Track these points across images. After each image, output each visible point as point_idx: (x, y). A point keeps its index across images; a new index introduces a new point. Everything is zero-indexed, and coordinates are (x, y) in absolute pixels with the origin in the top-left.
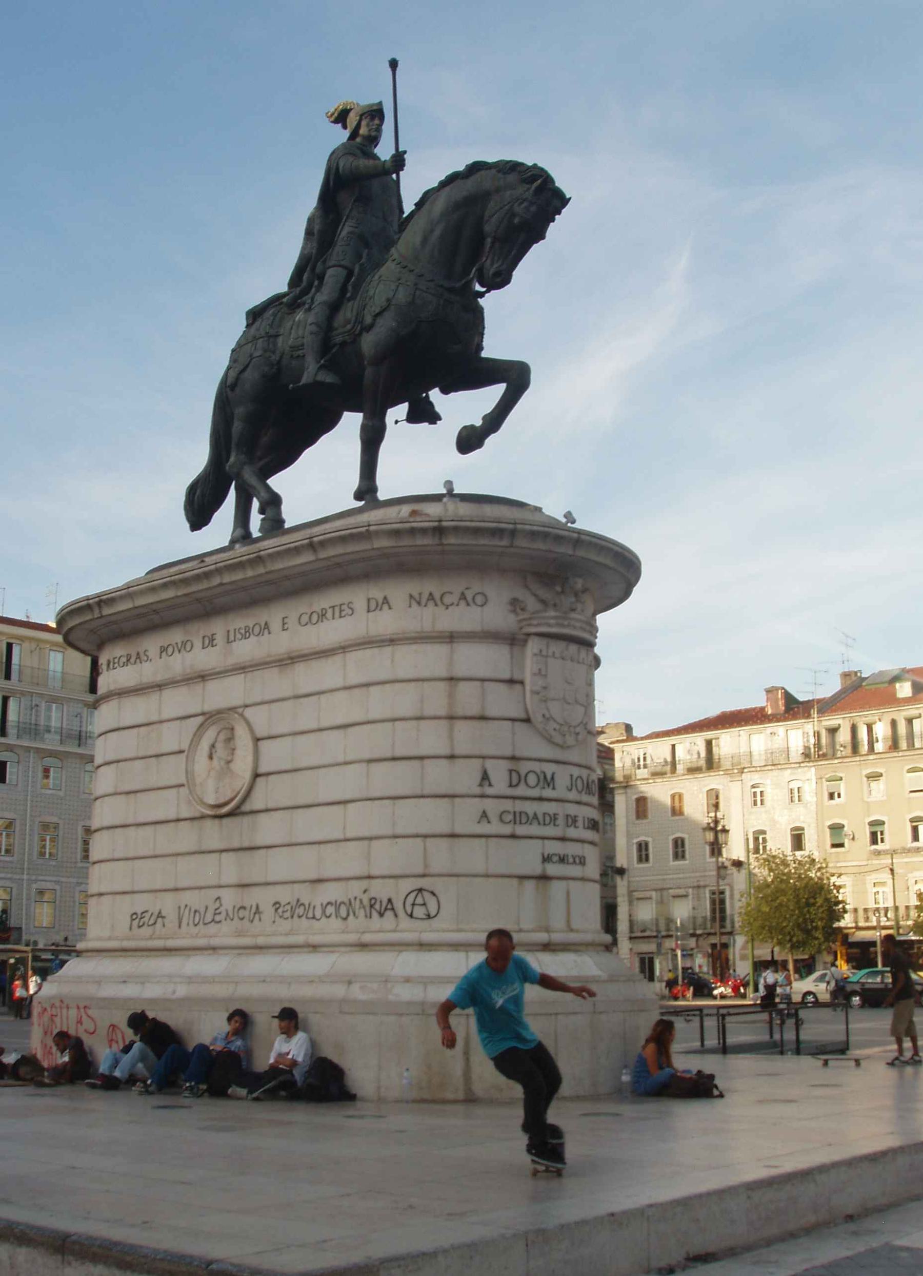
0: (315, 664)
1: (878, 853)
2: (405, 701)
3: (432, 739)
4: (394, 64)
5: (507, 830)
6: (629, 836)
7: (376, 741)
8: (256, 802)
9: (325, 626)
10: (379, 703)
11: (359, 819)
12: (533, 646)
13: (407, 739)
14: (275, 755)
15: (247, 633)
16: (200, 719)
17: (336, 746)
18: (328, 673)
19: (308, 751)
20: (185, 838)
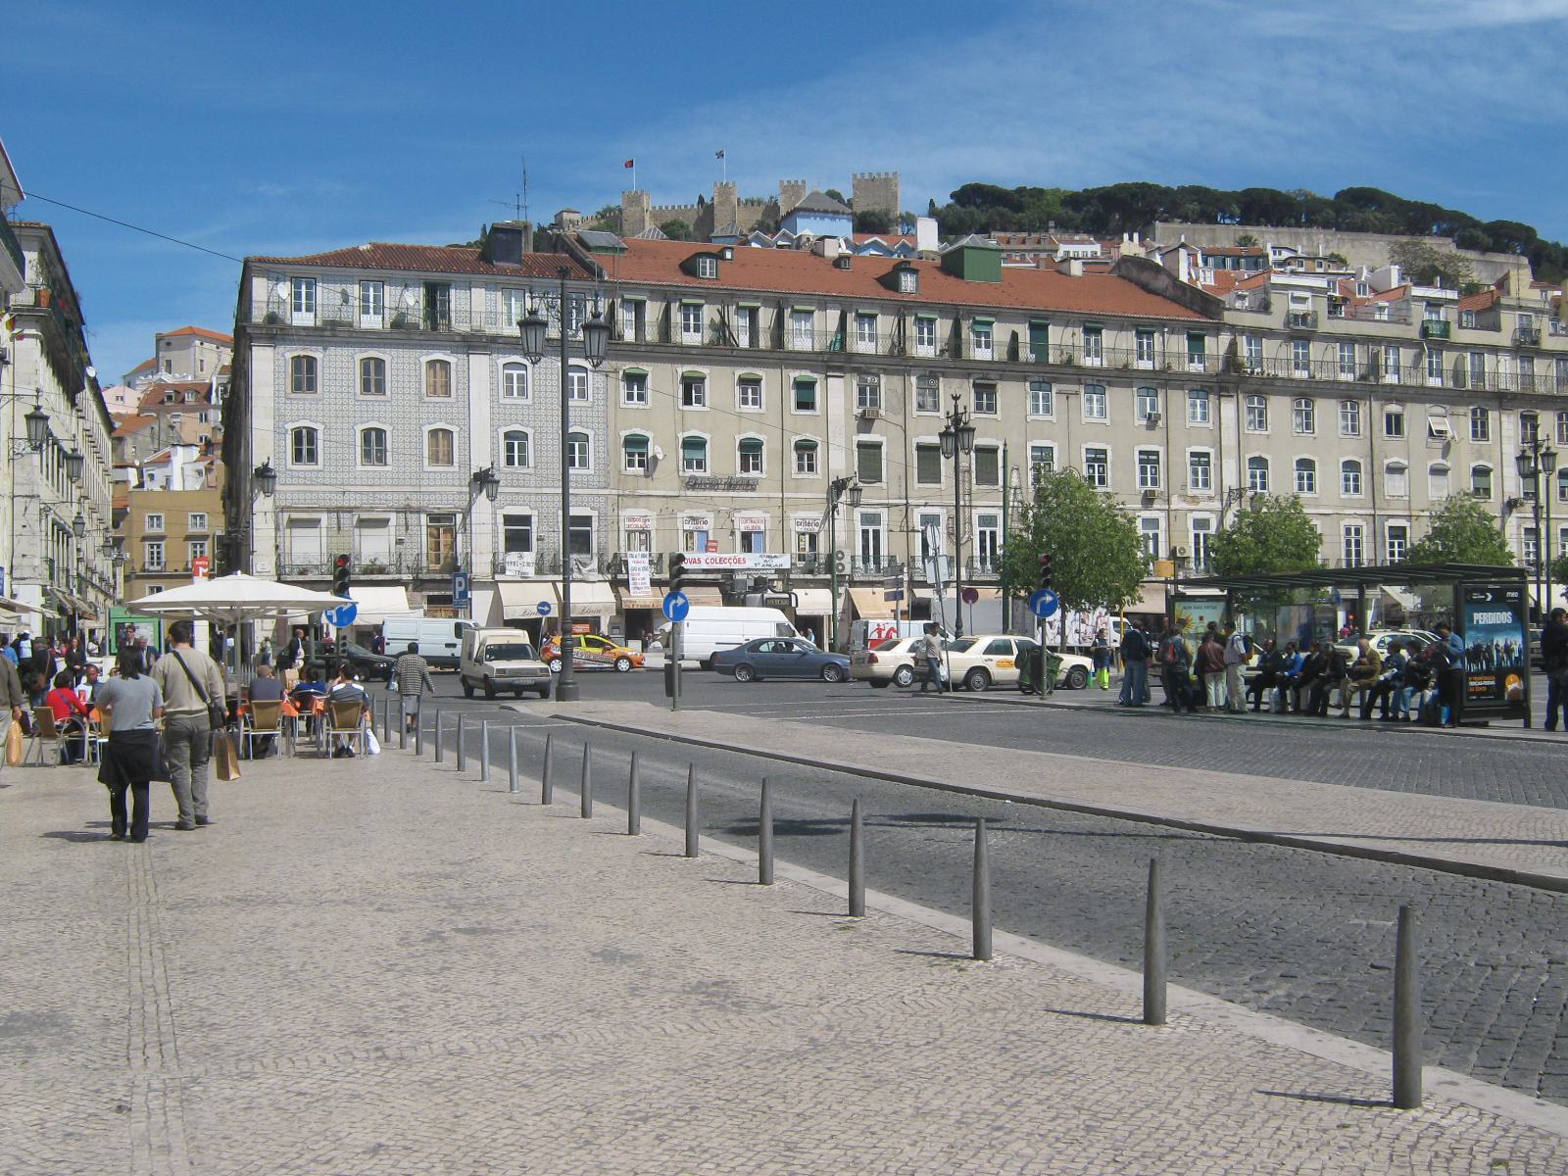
1: (693, 484)
6: (279, 417)
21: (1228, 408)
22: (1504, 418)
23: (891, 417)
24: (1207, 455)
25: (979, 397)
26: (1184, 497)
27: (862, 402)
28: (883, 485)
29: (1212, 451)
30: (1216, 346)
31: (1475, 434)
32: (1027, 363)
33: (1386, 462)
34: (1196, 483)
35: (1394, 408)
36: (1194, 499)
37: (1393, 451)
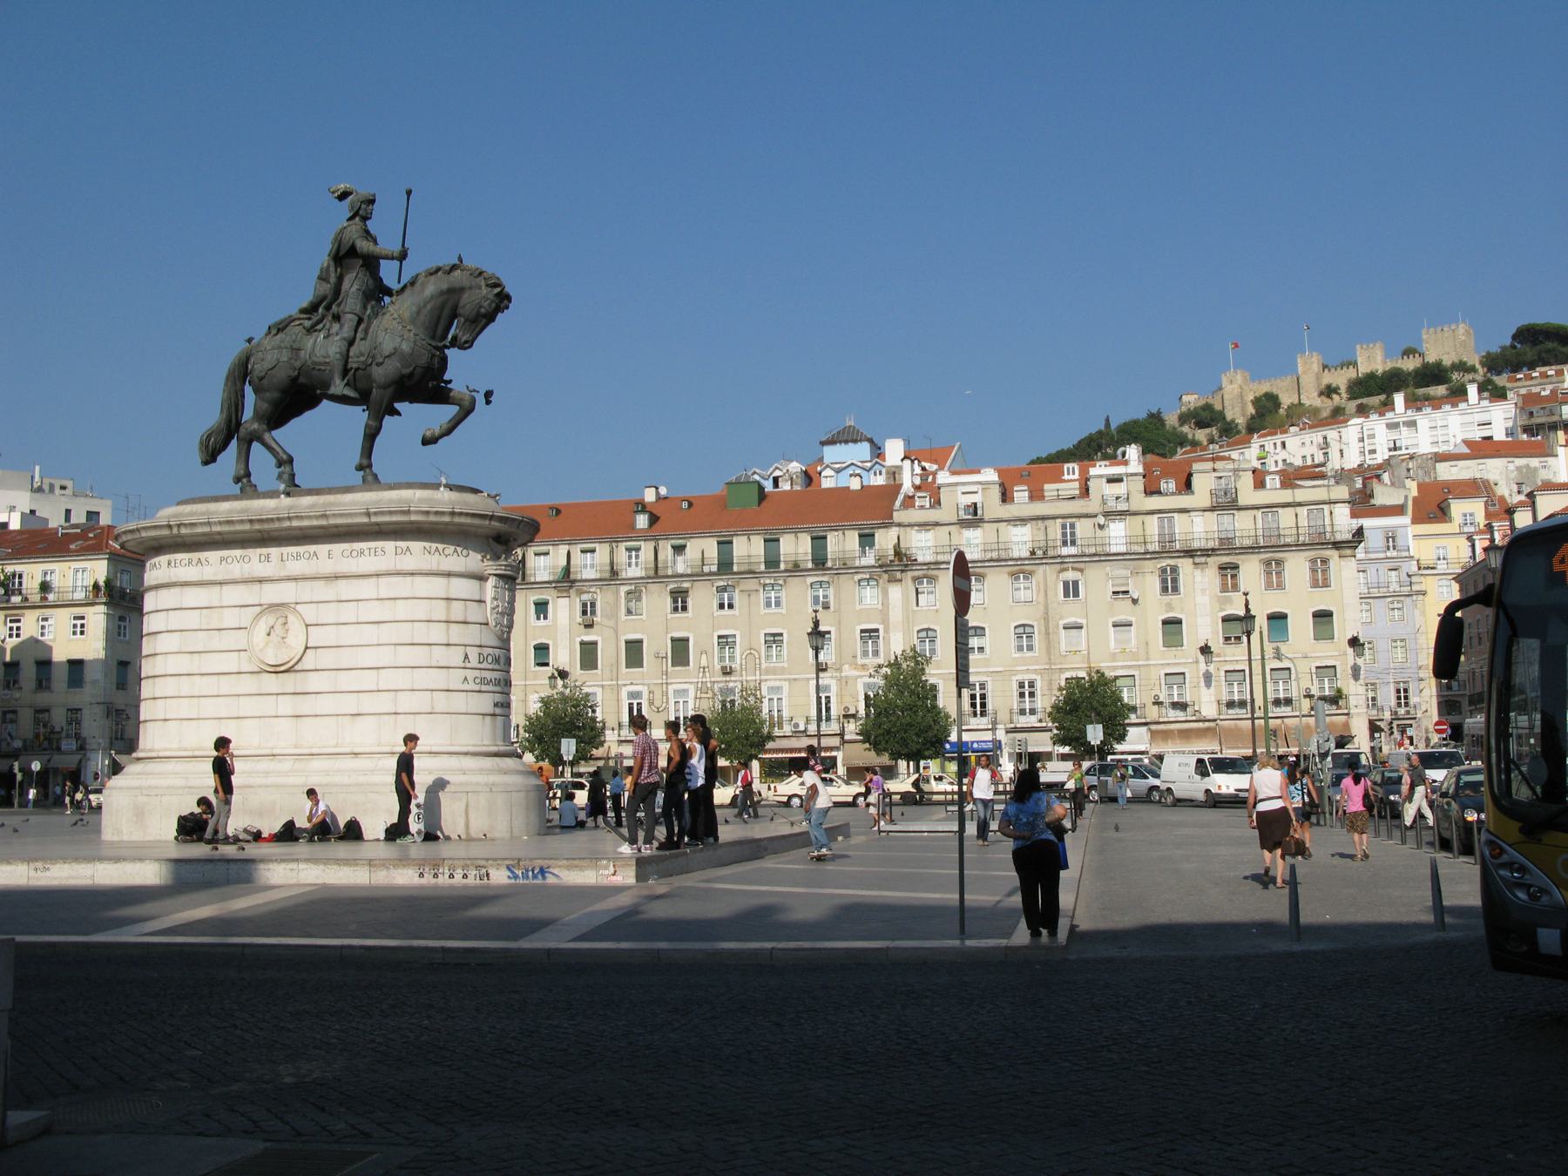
0: (354, 581)
2: (421, 610)
3: (437, 633)
4: (409, 193)
5: (477, 688)
7: (404, 633)
8: (308, 662)
9: (362, 560)
10: (402, 610)
11: (388, 679)
12: (492, 581)
13: (422, 633)
14: (317, 637)
15: (298, 557)
16: (258, 609)
17: (370, 634)
18: (366, 588)
19: (348, 635)
20: (248, 684)
21: (895, 592)
22: (1198, 572)
23: (606, 622)
24: (877, 630)
25: (675, 601)
26: (856, 666)
27: (584, 613)
28: (599, 672)
29: (881, 628)
30: (886, 540)
31: (1165, 590)
32: (711, 574)
33: (1062, 623)
34: (865, 654)
35: (1070, 575)
36: (864, 667)
37: (1071, 612)
